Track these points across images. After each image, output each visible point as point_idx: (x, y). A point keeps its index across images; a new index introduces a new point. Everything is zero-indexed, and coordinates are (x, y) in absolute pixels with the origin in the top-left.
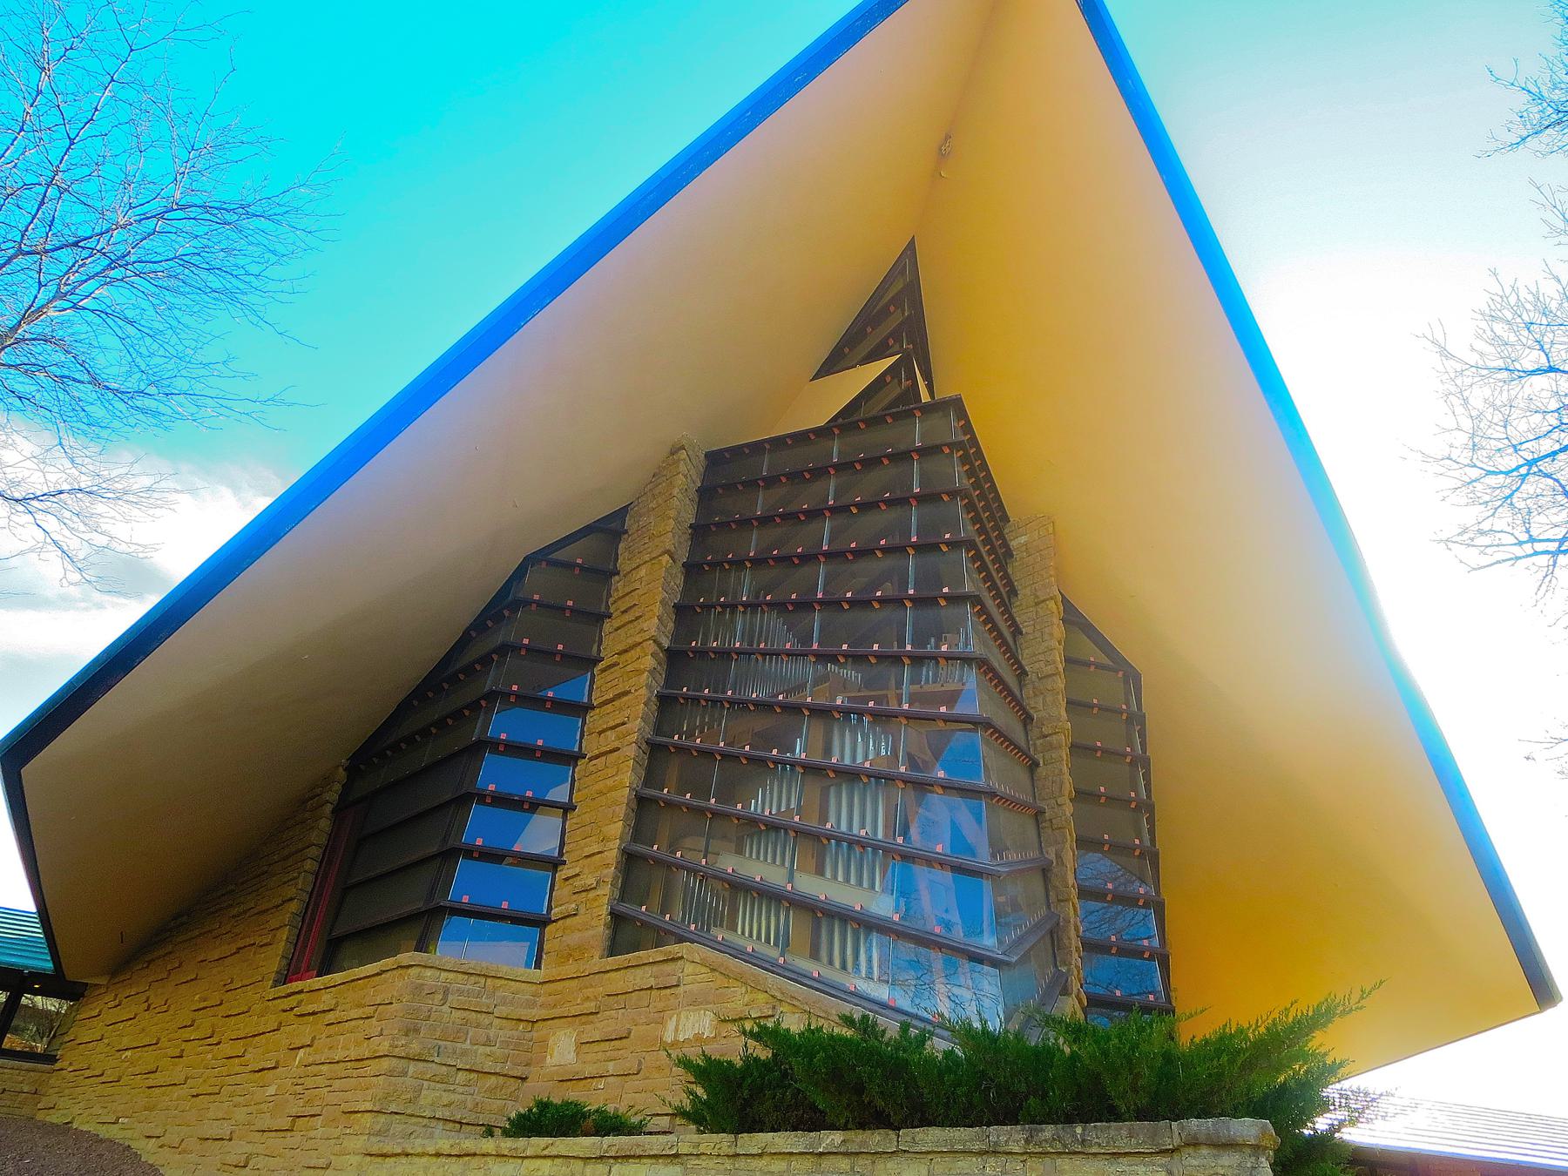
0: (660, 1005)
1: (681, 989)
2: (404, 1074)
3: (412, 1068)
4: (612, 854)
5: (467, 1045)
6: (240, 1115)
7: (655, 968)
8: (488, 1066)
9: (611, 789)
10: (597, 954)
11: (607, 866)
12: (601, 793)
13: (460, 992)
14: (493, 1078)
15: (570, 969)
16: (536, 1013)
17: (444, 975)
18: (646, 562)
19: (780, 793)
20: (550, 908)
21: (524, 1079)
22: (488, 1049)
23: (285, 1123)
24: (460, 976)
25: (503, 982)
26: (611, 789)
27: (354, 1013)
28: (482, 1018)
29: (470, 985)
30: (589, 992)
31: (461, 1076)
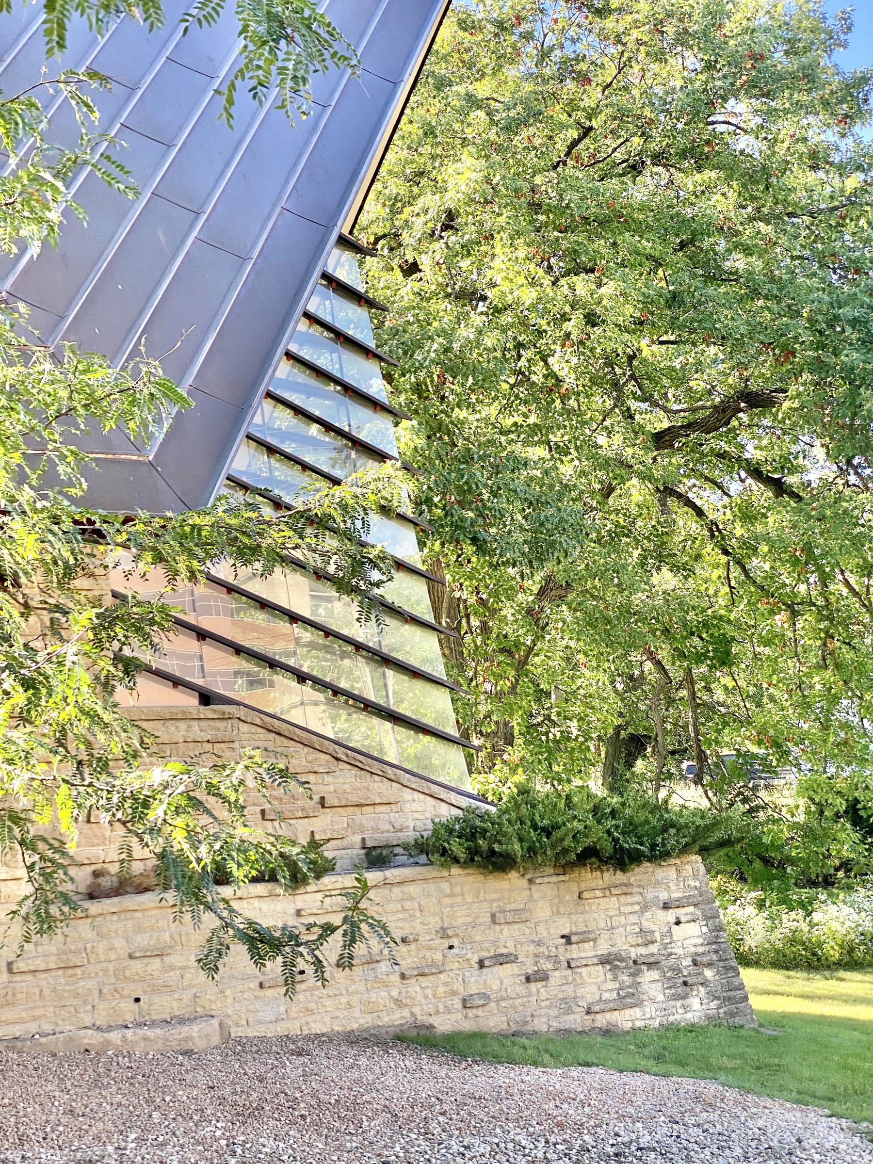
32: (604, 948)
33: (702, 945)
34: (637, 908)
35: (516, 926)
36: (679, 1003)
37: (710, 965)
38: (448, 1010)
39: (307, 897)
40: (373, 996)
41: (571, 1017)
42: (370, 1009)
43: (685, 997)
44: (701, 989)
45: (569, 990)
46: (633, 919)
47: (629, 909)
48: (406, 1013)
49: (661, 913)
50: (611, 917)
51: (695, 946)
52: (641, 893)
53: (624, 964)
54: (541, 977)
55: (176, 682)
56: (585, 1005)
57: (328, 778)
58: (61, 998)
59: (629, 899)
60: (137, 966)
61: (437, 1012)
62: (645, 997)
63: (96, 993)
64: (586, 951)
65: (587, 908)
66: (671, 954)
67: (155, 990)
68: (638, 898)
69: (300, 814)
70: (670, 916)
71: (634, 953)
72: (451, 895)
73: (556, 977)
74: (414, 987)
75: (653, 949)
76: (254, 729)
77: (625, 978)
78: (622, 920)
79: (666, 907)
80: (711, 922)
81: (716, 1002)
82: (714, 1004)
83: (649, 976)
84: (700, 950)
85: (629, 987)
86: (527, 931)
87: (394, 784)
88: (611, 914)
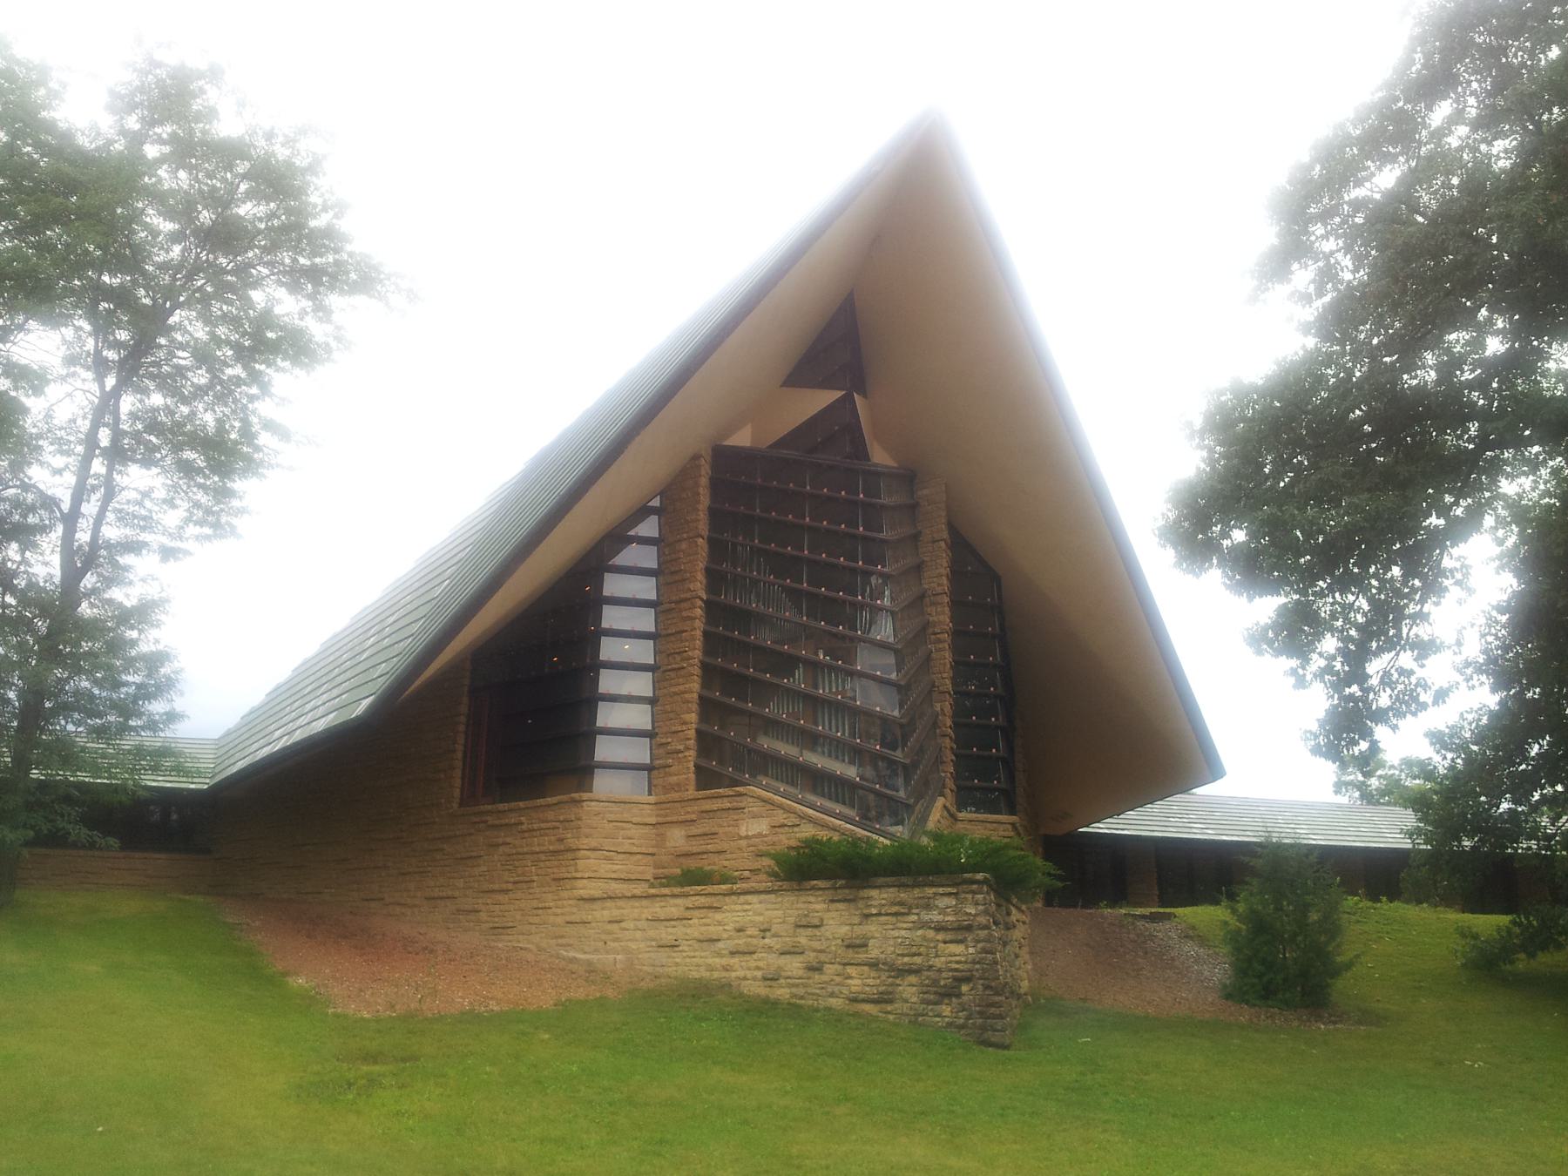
0: (736, 817)
1: (746, 810)
2: (589, 858)
4: (692, 733)
5: (620, 840)
6: (460, 883)
7: (730, 798)
8: (635, 849)
9: (685, 692)
10: (692, 787)
11: (689, 739)
12: (676, 694)
13: (611, 812)
15: (675, 796)
16: (653, 820)
17: (602, 804)
18: (685, 539)
19: (788, 705)
23: (510, 886)
25: (632, 805)
26: (685, 692)
27: (543, 825)
30: (689, 809)
33: (966, 962)
36: (930, 1007)
40: (710, 961)
42: (711, 969)
44: (954, 1000)
47: (905, 926)
49: (931, 934)
52: (917, 914)
60: (609, 927)
66: (931, 966)
67: (616, 940)
68: (915, 918)
70: (940, 937)
73: (830, 969)
74: (735, 961)
76: (755, 800)
80: (980, 945)
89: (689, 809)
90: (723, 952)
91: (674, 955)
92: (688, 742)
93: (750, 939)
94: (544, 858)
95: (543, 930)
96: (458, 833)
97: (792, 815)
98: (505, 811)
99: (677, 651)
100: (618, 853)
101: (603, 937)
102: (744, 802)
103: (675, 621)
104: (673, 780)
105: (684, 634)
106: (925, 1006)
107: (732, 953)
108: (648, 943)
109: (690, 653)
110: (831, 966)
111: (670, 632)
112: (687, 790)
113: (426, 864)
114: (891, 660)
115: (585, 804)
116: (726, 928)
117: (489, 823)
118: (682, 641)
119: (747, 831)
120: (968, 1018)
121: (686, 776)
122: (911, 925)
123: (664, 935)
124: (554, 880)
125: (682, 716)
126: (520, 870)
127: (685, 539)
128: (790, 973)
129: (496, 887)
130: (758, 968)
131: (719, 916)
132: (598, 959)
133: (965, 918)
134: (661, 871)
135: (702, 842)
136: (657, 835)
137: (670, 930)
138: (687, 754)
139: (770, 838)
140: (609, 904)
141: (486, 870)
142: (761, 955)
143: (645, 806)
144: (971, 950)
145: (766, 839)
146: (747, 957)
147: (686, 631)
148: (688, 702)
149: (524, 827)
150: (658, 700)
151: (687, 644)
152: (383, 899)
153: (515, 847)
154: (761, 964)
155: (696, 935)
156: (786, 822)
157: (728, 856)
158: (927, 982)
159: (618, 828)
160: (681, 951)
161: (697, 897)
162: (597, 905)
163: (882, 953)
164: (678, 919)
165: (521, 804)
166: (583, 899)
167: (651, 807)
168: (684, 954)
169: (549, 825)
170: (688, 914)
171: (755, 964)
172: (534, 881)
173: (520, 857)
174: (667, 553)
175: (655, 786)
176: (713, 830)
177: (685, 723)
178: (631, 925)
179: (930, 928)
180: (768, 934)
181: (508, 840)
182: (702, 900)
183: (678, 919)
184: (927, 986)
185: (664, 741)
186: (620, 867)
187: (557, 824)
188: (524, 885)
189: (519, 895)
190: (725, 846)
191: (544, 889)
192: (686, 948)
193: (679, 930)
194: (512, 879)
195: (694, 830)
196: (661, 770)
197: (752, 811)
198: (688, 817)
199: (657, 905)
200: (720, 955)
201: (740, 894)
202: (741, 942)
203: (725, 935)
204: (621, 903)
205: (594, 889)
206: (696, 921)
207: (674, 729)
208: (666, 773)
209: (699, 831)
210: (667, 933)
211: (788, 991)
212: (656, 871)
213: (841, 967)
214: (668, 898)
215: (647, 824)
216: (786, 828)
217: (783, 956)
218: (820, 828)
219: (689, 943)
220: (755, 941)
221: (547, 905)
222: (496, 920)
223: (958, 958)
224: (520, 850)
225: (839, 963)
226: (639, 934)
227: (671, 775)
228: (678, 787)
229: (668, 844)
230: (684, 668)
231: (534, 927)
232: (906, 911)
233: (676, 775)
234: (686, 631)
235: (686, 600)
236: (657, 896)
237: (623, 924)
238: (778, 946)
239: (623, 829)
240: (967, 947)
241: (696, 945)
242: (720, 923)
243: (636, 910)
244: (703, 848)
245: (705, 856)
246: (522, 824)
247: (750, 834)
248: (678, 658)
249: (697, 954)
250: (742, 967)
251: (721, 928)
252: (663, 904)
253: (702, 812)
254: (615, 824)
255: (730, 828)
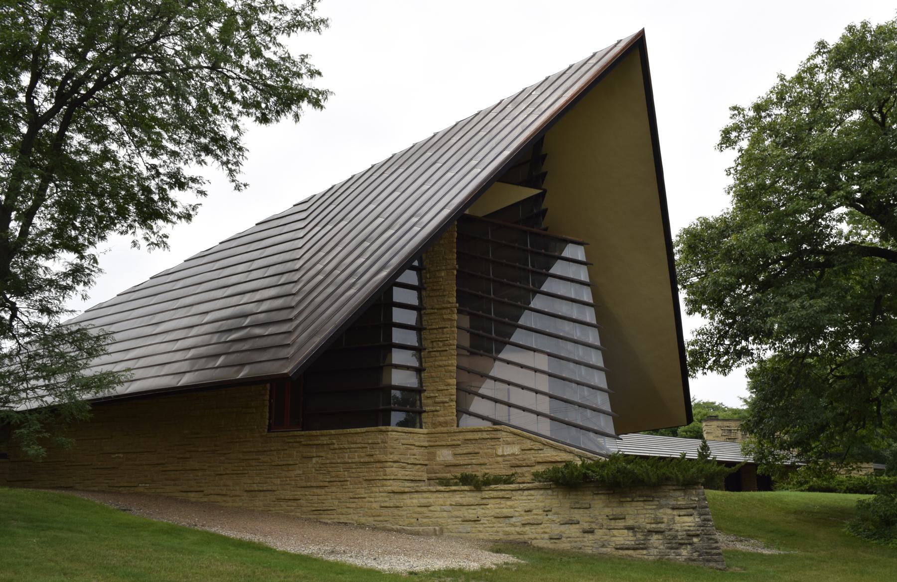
0: (493, 444)
1: (501, 440)
2: (392, 467)
3: (395, 465)
7: (488, 432)
8: (417, 462)
9: (446, 366)
11: (453, 395)
12: (440, 366)
13: (403, 439)
14: (419, 466)
16: (426, 444)
18: (443, 270)
20: (421, 407)
21: (426, 465)
22: (415, 457)
23: (327, 484)
24: (403, 434)
26: (449, 366)
28: (413, 447)
29: (404, 435)
30: (455, 438)
31: (410, 466)
32: (630, 522)
33: (694, 526)
34: (654, 507)
35: (582, 510)
36: (672, 551)
37: (697, 536)
38: (542, 539)
39: (487, 492)
40: (507, 529)
41: (605, 549)
43: (677, 549)
44: (689, 546)
45: (606, 538)
46: (653, 512)
47: (650, 507)
48: (521, 537)
49: (669, 511)
50: (637, 510)
51: (689, 526)
52: (658, 501)
53: (640, 530)
54: (591, 532)
55: (484, 418)
56: (614, 545)
57: (540, 452)
58: (394, 516)
59: (650, 503)
60: (419, 509)
61: (536, 539)
62: (649, 546)
63: (405, 517)
64: (621, 524)
65: (624, 505)
67: (426, 517)
69: (524, 465)
70: (676, 512)
71: (648, 526)
72: (553, 495)
73: (599, 533)
74: (527, 528)
75: (662, 526)
76: (508, 434)
77: (639, 536)
78: (645, 512)
79: (673, 509)
80: (702, 517)
81: (697, 553)
82: (696, 554)
83: (655, 539)
84: (692, 528)
85: (642, 540)
86: (588, 512)
87: (571, 454)
88: (638, 508)
89: (455, 438)
90: (517, 524)
91: (477, 526)
92: (452, 397)
93: (536, 517)
94: (354, 466)
95: (361, 512)
96: (272, 448)
97: (537, 443)
98: (317, 436)
99: (441, 339)
100: (408, 464)
101: (415, 516)
102: (499, 434)
103: (437, 320)
104: (442, 419)
105: (445, 330)
106: (669, 550)
107: (524, 525)
108: (454, 519)
109: (451, 342)
110: (599, 530)
111: (434, 327)
112: (452, 426)
113: (241, 468)
114: (599, 354)
115: (389, 433)
116: (516, 509)
117: (303, 443)
118: (443, 333)
119: (503, 452)
120: (699, 556)
121: (451, 418)
122: (654, 507)
123: (466, 514)
124: (366, 480)
125: (446, 380)
126: (333, 474)
127: (443, 270)
128: (570, 535)
129: (314, 484)
130: (545, 533)
131: (509, 503)
132: (423, 530)
133: (692, 502)
134: (433, 475)
135: (466, 458)
136: (428, 453)
137: (470, 511)
138: (451, 404)
139: (520, 456)
140: (416, 495)
141: (301, 472)
142: (546, 525)
143: (422, 435)
144: (697, 520)
145: (517, 457)
146: (536, 527)
147: (447, 327)
148: (450, 372)
149: (336, 446)
150: (425, 370)
151: (448, 336)
152: (203, 491)
153: (328, 459)
154: (547, 530)
155: (493, 514)
156: (533, 447)
157: (489, 467)
158: (669, 537)
159: (407, 449)
160: (482, 524)
161: (490, 492)
162: (405, 496)
163: (636, 522)
164: (477, 505)
165: (333, 432)
166: (394, 492)
167: (424, 436)
168: (485, 525)
169: (359, 445)
170: (484, 501)
171: (542, 531)
172: (347, 481)
173: (333, 465)
174: (428, 277)
175: (425, 423)
176: (476, 451)
177: (449, 385)
178: (438, 508)
179: (668, 508)
180: (550, 513)
181: (322, 454)
182: (494, 494)
183: (477, 505)
184: (670, 539)
185: (432, 395)
186: (410, 473)
187: (366, 445)
188: (339, 484)
189: (334, 489)
190: (486, 461)
191: (356, 486)
192: (486, 522)
193: (480, 511)
194: (328, 480)
195: (459, 450)
196: (430, 413)
197: (507, 441)
198: (454, 442)
199: (457, 496)
200: (514, 525)
201: (525, 490)
202: (528, 518)
203: (517, 514)
204: (425, 495)
205: (396, 486)
206: (492, 506)
207: (440, 388)
208: (434, 415)
209: (465, 451)
210: (471, 513)
211: (569, 545)
212: (429, 475)
213: (608, 531)
214: (466, 492)
215: (422, 447)
216: (533, 451)
217: (563, 526)
218: (559, 451)
219: (488, 519)
220: (540, 517)
221: (362, 496)
222: (316, 505)
223: (690, 524)
224: (334, 461)
225: (607, 529)
226: (445, 514)
227: (438, 416)
228: (446, 424)
229: (438, 458)
230: (447, 351)
231: (352, 509)
232: (651, 499)
233: (443, 416)
234: (447, 327)
235: (447, 308)
236: (458, 491)
237: (431, 508)
238: (558, 520)
239: (411, 449)
240: (694, 518)
241: (494, 520)
242: (511, 507)
243: (440, 500)
244: (469, 462)
245: (470, 467)
246: (334, 444)
247: (505, 454)
248: (441, 344)
249: (495, 525)
250: (532, 532)
251: (512, 510)
252: (462, 496)
253: (466, 440)
254: (406, 446)
255: (489, 450)
